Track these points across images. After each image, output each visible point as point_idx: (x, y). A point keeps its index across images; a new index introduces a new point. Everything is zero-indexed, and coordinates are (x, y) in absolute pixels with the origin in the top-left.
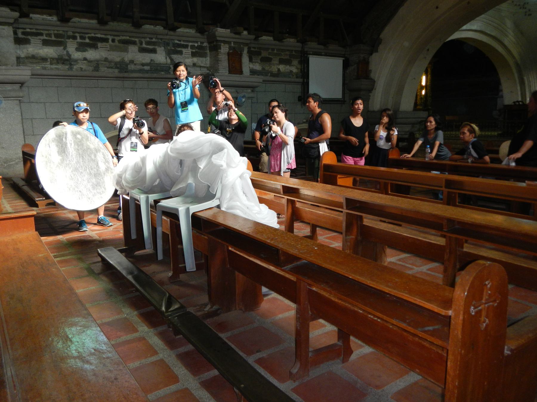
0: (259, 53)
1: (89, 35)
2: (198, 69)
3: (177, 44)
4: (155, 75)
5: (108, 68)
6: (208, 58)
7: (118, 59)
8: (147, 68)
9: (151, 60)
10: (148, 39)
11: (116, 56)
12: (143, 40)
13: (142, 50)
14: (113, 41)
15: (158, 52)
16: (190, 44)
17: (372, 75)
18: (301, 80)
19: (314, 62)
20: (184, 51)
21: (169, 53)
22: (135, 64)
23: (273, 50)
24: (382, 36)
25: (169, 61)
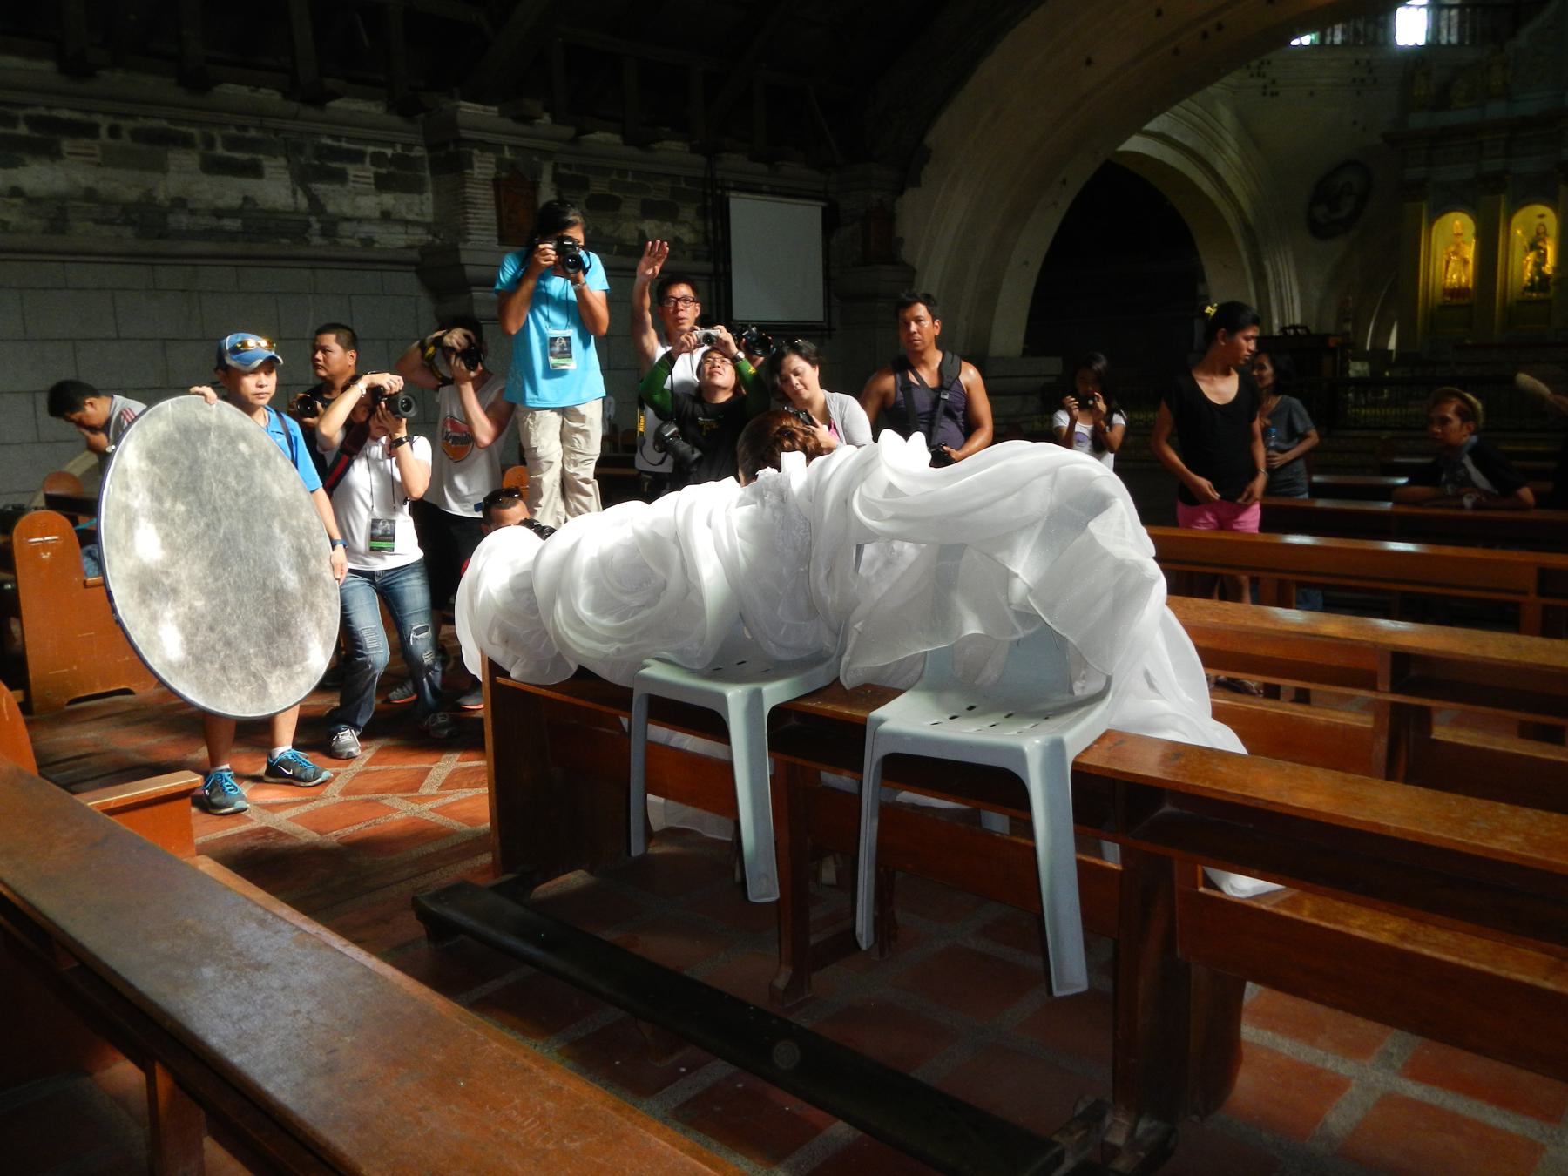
0: (582, 184)
1: (29, 111)
2: (399, 229)
3: (330, 148)
4: (260, 248)
5: (96, 221)
6: (429, 195)
7: (132, 195)
8: (231, 224)
9: (246, 199)
10: (233, 131)
11: (123, 185)
12: (215, 133)
13: (214, 166)
14: (114, 132)
15: (267, 171)
16: (371, 149)
17: (905, 253)
18: (708, 267)
19: (745, 211)
20: (352, 170)
21: (302, 178)
22: (193, 212)
23: (623, 173)
24: (931, 139)
25: (303, 203)
